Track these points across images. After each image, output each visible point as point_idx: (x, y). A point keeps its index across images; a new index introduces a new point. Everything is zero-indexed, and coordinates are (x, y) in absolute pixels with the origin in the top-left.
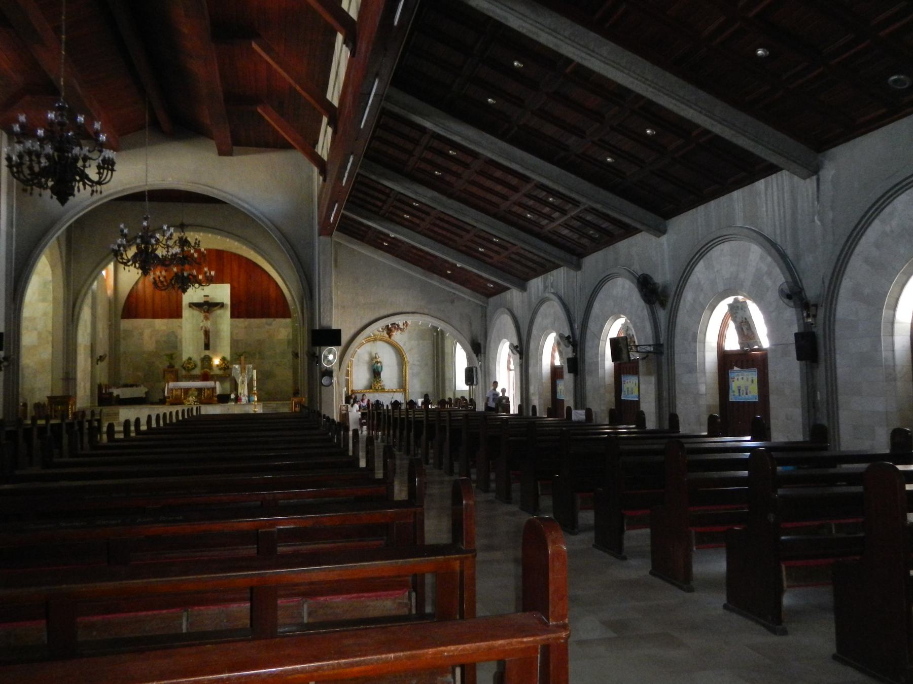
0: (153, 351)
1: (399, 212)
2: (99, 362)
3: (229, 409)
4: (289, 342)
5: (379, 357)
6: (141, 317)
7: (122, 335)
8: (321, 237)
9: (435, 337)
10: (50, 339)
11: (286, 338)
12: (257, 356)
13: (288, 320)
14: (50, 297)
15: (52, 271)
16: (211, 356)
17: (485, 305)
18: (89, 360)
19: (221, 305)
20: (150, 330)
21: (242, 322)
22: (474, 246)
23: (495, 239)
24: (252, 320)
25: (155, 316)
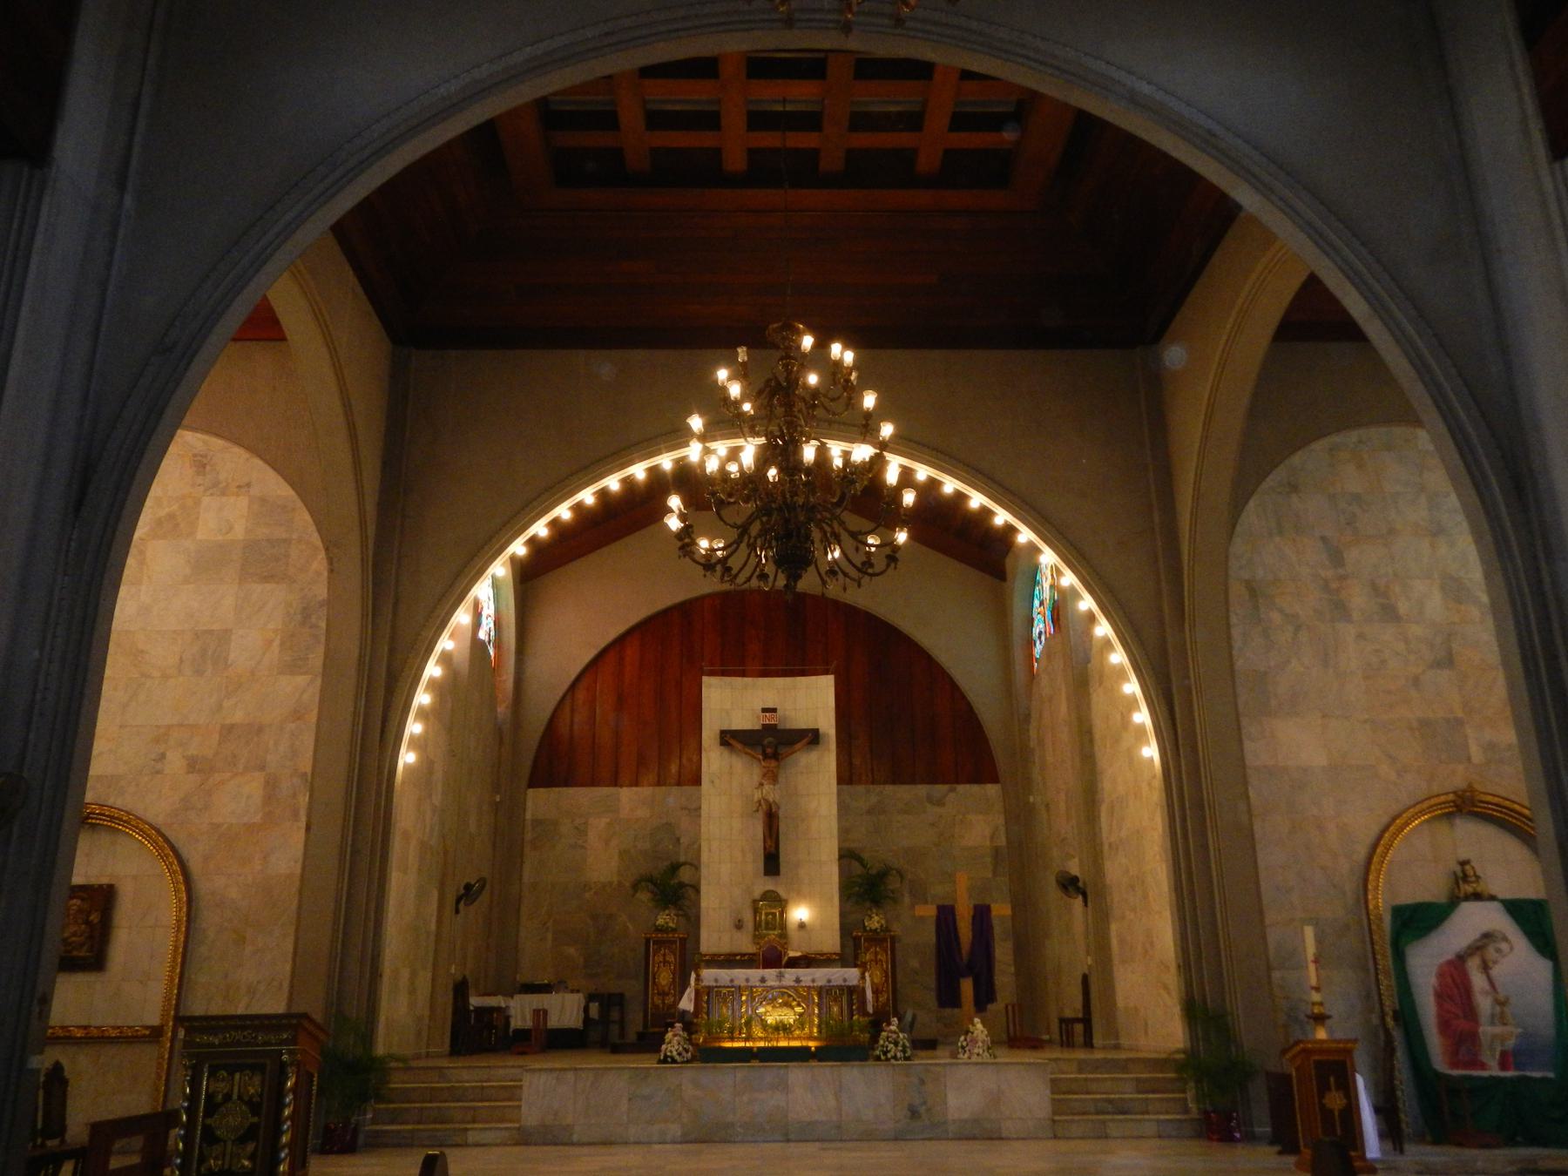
0: (611, 883)
2: (462, 905)
3: (922, 1082)
4: (997, 852)
5: (1478, 878)
7: (528, 836)
10: (303, 800)
12: (907, 899)
13: (992, 790)
14: (317, 658)
15: (330, 561)
16: (783, 894)
18: (435, 894)
19: (812, 737)
20: (604, 821)
21: (868, 796)
24: (889, 789)
25: (615, 782)
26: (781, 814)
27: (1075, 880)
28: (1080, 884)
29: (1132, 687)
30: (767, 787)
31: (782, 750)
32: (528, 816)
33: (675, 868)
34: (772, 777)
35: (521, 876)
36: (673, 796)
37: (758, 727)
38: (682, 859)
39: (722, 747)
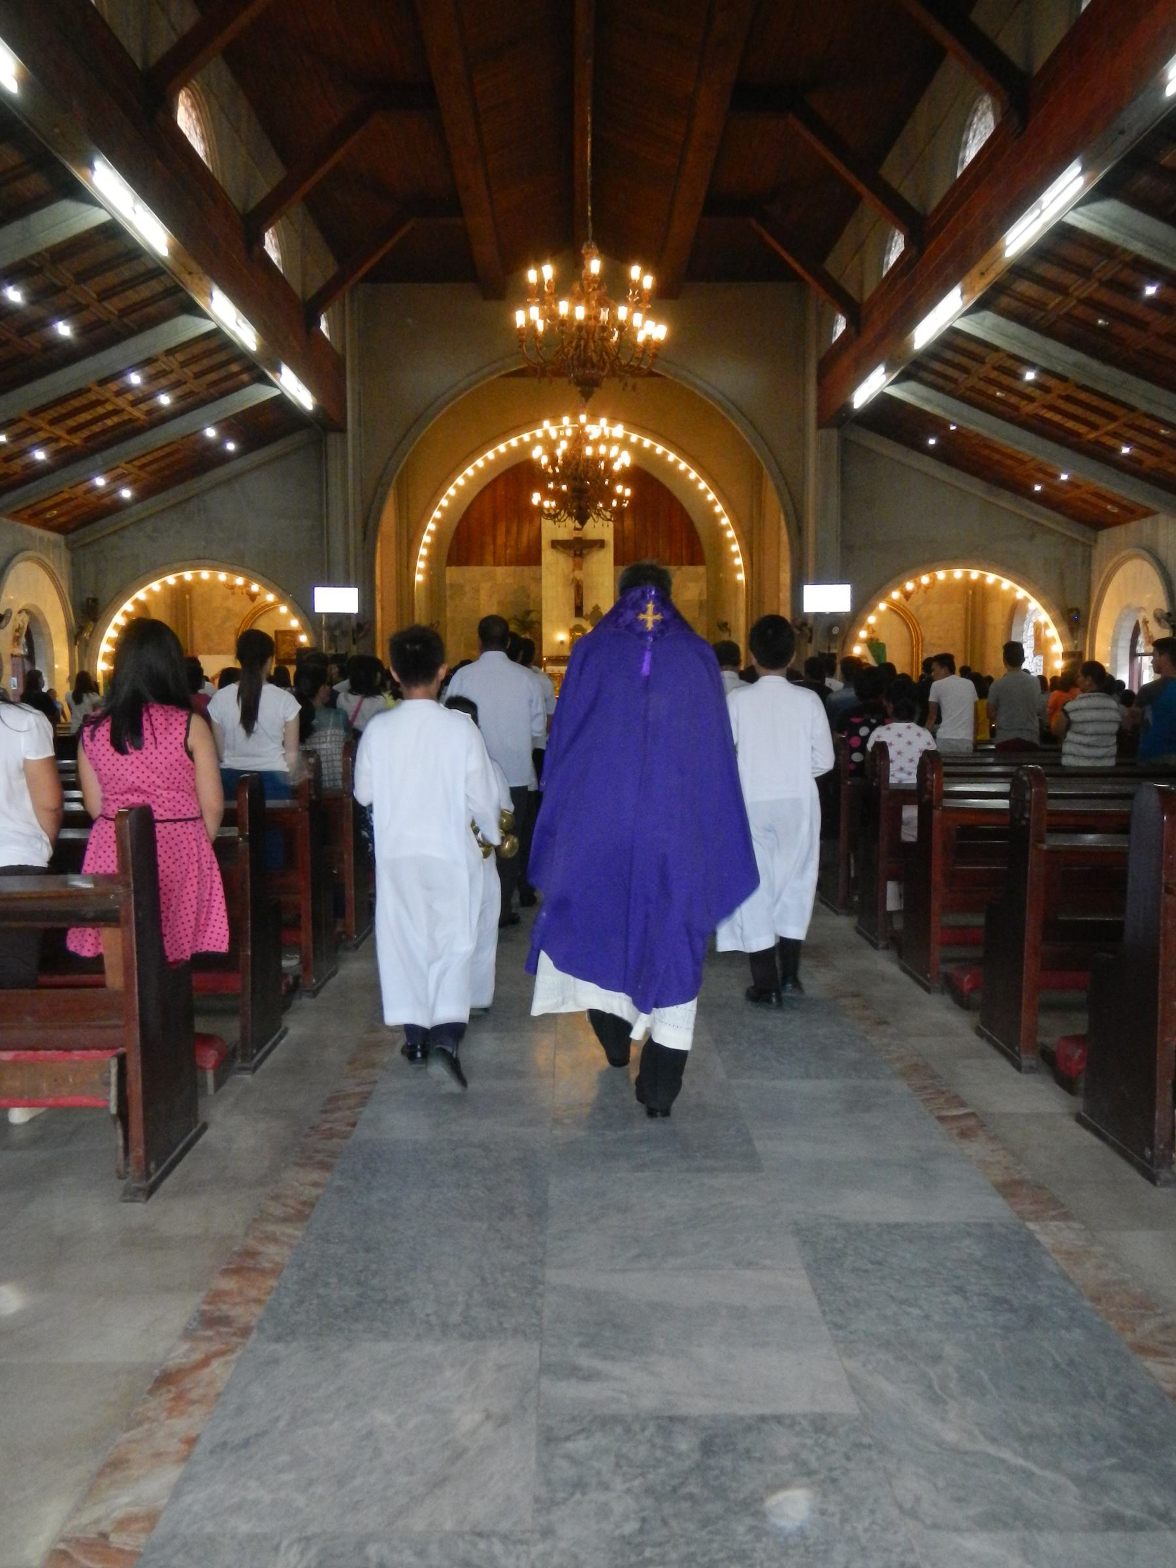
1: (991, 390)
4: (701, 602)
6: (477, 565)
7: (448, 593)
8: (823, 432)
9: (970, 598)
11: (697, 598)
13: (701, 569)
17: (1092, 543)
19: (601, 544)
22: (1111, 442)
23: (1163, 431)
25: (497, 563)
26: (584, 585)
27: (725, 624)
28: (728, 626)
29: (735, 548)
30: (577, 572)
31: (585, 552)
32: (448, 582)
33: (528, 613)
34: (578, 566)
35: (445, 617)
36: (528, 571)
37: (572, 538)
38: (531, 609)
39: (552, 550)
